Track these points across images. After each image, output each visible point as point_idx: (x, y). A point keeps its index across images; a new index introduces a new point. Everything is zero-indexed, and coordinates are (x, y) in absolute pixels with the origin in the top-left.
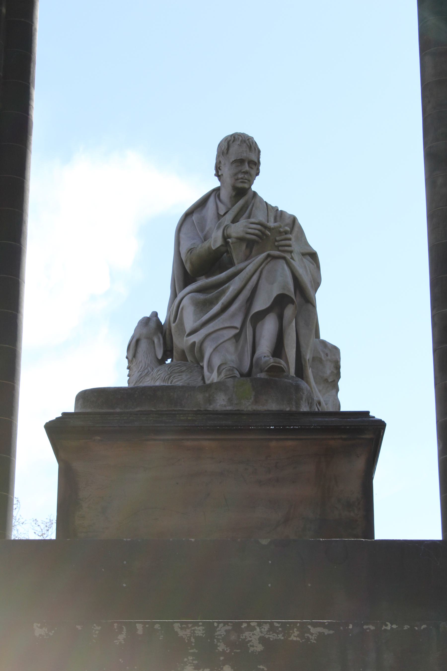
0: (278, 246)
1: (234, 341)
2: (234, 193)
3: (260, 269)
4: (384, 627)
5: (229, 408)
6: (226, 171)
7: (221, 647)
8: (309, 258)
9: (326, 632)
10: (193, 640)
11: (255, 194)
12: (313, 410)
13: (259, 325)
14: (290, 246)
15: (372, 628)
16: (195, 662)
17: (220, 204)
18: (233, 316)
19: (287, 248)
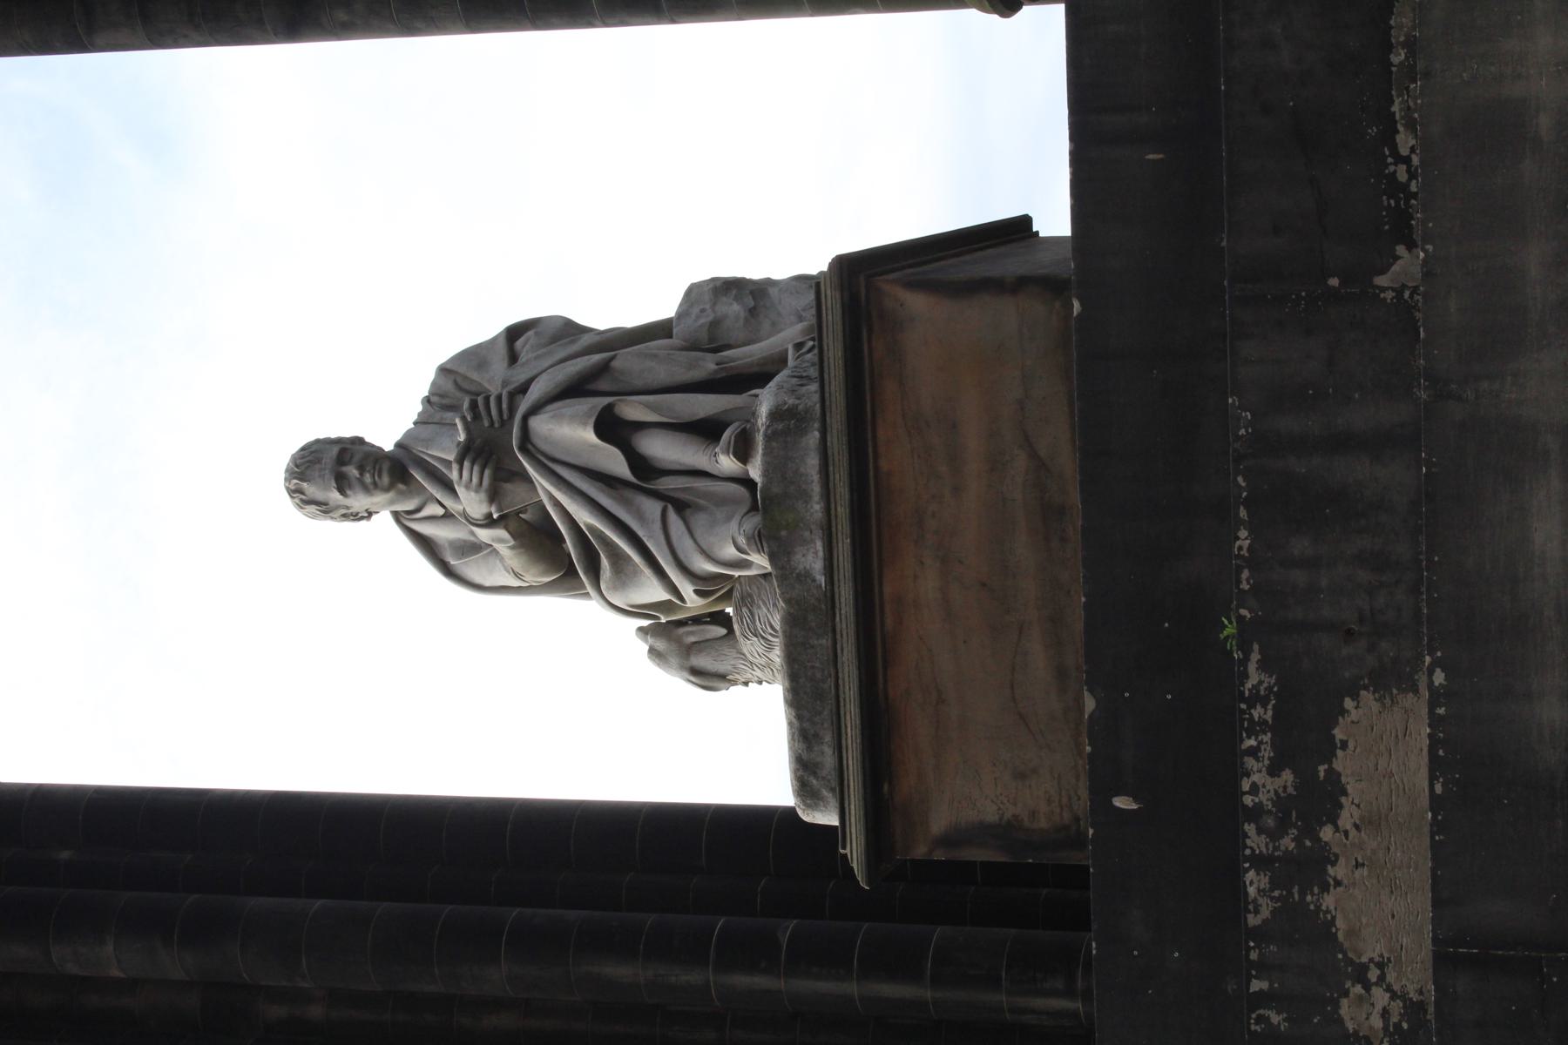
0: (503, 423)
1: (688, 512)
2: (401, 486)
3: (550, 464)
4: (1244, 552)
5: (819, 545)
6: (358, 501)
7: (1287, 843)
8: (519, 344)
9: (1255, 656)
10: (1276, 893)
11: (399, 445)
12: (814, 372)
13: (658, 465)
14: (499, 398)
15: (1245, 574)
16: (1316, 890)
17: (426, 512)
18: (641, 517)
19: (504, 406)
